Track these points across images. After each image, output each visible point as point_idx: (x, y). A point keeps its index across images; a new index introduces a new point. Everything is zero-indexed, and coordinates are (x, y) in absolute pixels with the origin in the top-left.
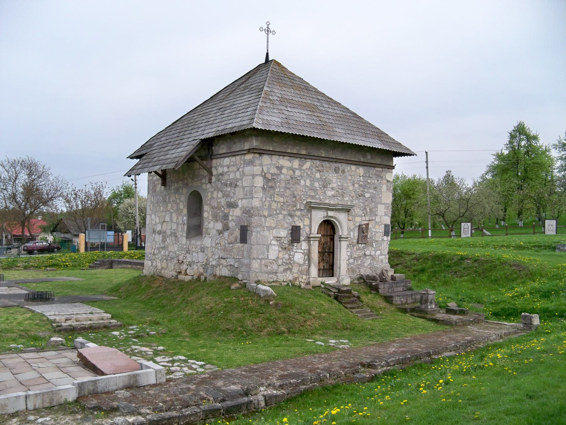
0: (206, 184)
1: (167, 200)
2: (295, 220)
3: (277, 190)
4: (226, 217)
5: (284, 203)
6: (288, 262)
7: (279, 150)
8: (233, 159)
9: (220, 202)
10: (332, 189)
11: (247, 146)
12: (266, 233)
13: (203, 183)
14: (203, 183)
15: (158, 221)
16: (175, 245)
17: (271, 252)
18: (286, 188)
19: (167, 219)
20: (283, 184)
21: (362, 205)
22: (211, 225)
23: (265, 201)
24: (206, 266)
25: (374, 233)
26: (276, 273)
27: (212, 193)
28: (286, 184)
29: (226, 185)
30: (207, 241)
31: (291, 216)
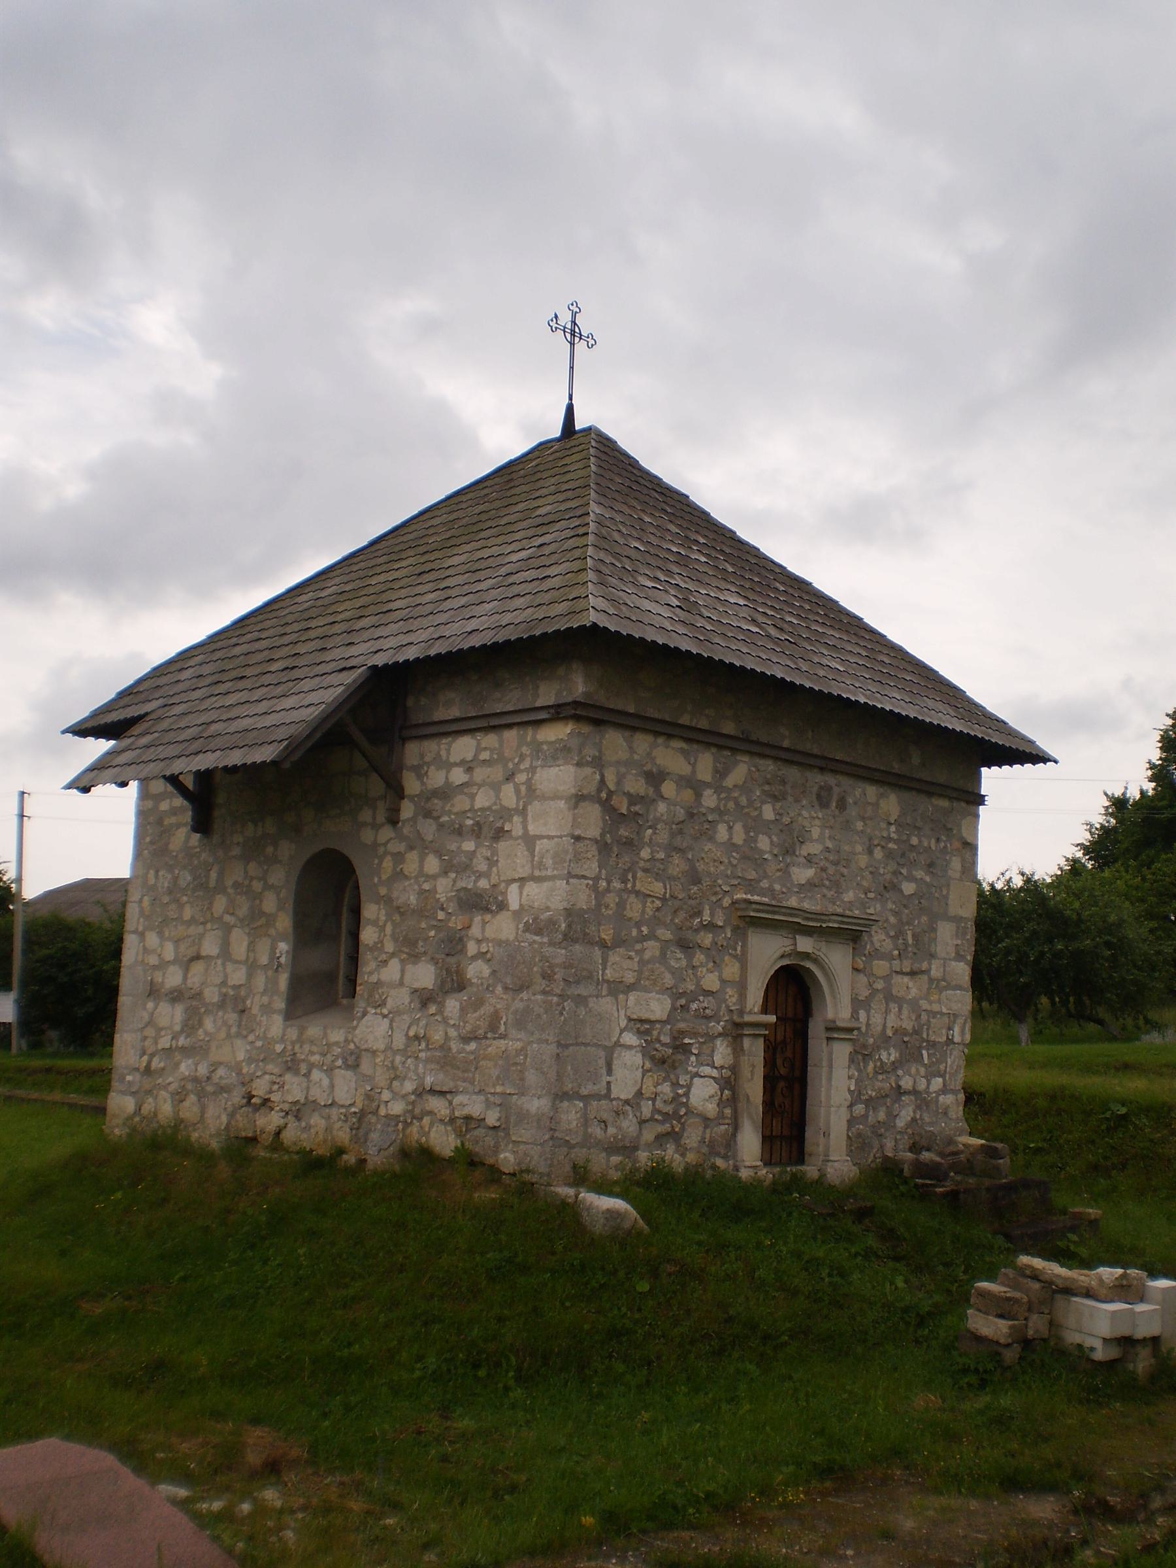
0: (376, 827)
1: (212, 884)
2: (696, 962)
3: (645, 853)
4: (454, 944)
5: (663, 899)
6: (669, 1109)
7: (656, 716)
8: (491, 740)
9: (434, 891)
10: (809, 860)
11: (547, 694)
12: (606, 1004)
13: (364, 824)
14: (364, 824)
15: (169, 952)
16: (239, 1042)
17: (619, 1072)
18: (672, 849)
19: (210, 947)
20: (663, 836)
21: (892, 920)
22: (395, 974)
23: (608, 890)
24: (361, 1119)
25: (924, 1017)
27: (399, 858)
28: (673, 835)
29: (459, 832)
30: (373, 1030)
31: (686, 946)
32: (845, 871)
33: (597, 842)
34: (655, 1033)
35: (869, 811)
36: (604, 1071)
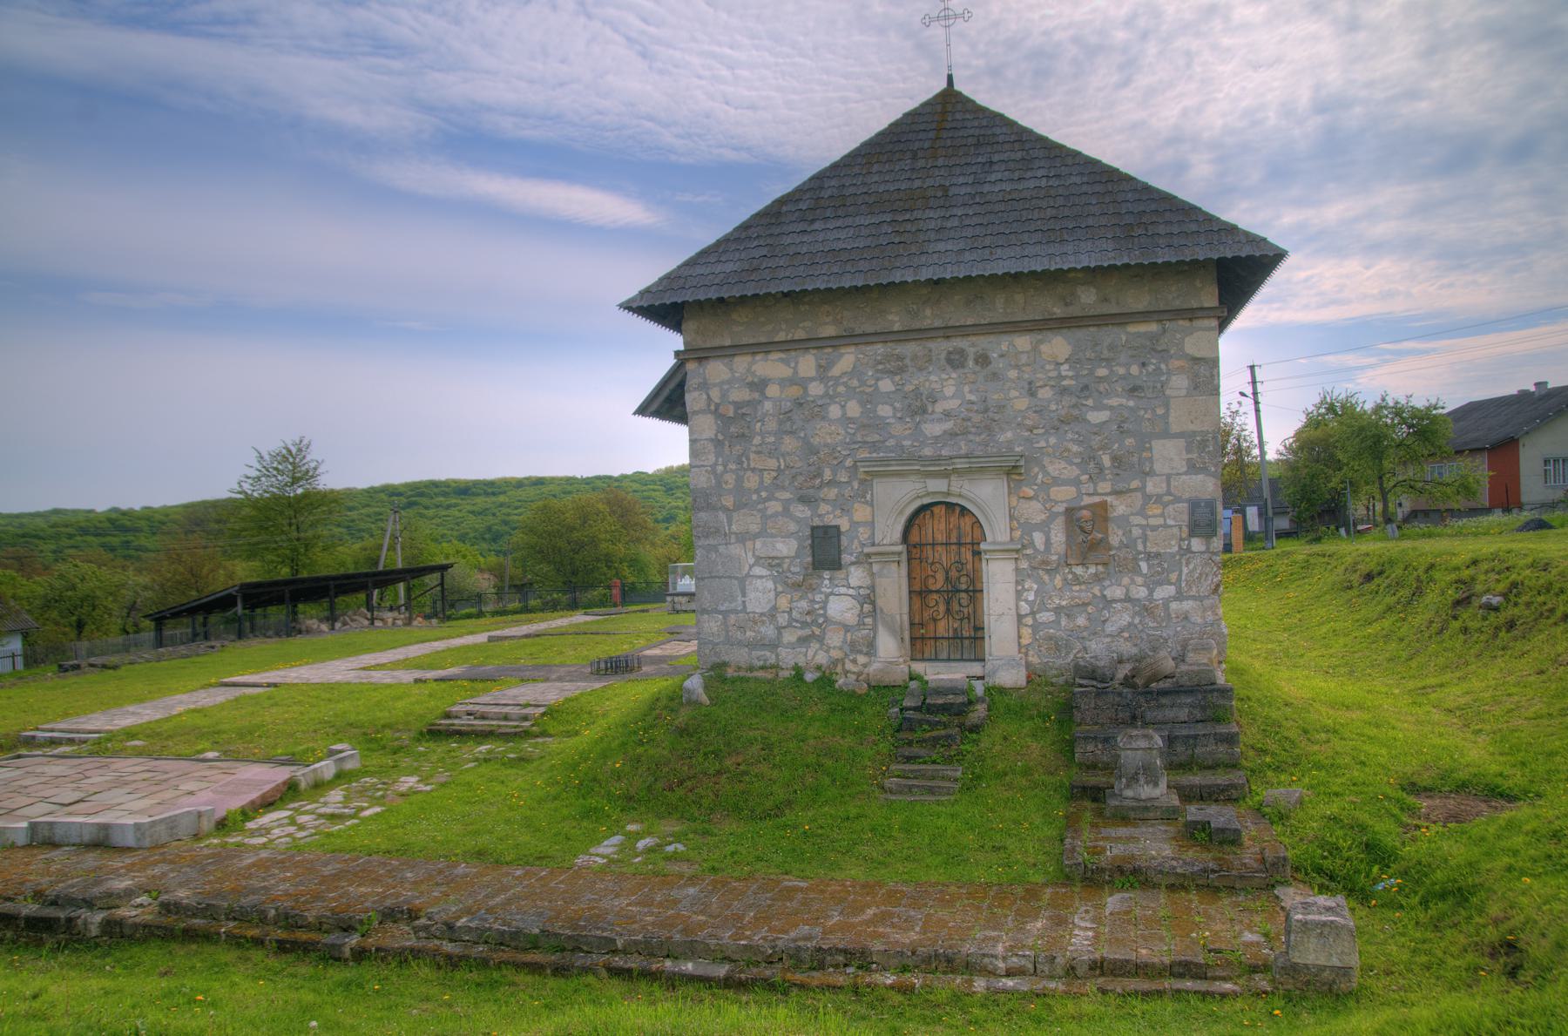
3: (757, 440)
5: (779, 470)
7: (752, 341)
12: (736, 550)
17: (751, 595)
20: (772, 425)
21: (1075, 448)
23: (725, 471)
25: (1136, 532)
26: (774, 646)
28: (781, 423)
31: (804, 500)
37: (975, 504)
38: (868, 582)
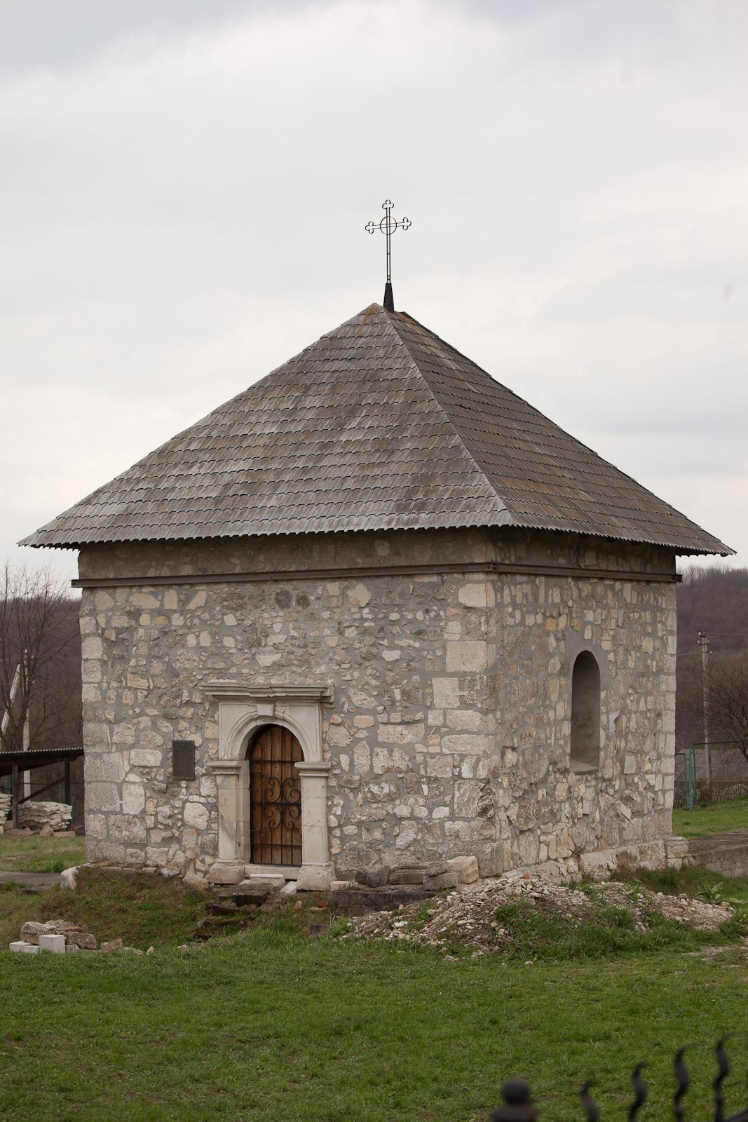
5: (148, 689)
6: (170, 822)
12: (115, 757)
17: (127, 798)
18: (151, 657)
20: (144, 650)
21: (373, 682)
23: (109, 688)
25: (419, 758)
26: (143, 845)
28: (151, 648)
31: (169, 717)
32: (313, 651)
33: (99, 660)
34: (153, 774)
35: (334, 602)
36: (117, 797)
37: (291, 724)
38: (213, 793)
